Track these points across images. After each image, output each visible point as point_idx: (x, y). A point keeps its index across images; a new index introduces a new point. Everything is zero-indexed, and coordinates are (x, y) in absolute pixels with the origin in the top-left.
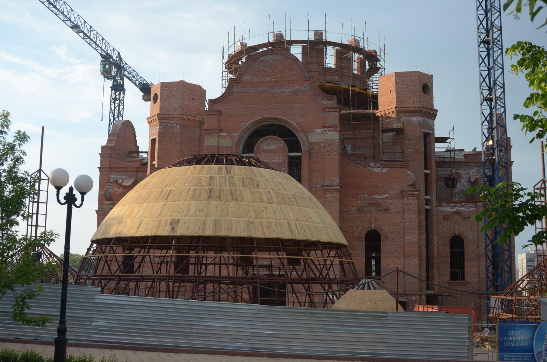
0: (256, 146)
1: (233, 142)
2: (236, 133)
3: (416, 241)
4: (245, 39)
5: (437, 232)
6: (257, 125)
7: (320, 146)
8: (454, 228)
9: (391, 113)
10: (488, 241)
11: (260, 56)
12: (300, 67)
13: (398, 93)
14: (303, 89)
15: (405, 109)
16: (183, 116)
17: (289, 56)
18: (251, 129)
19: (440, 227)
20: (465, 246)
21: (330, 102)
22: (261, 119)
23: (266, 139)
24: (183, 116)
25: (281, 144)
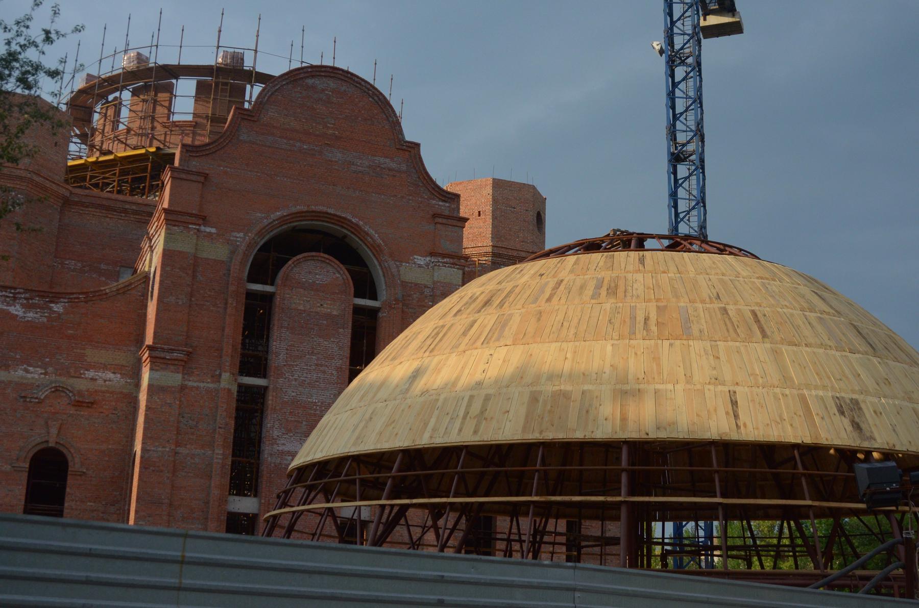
0: (343, 268)
1: (233, 252)
2: (239, 232)
4: (157, 46)
6: (290, 223)
7: (422, 293)
9: (480, 255)
11: (306, 75)
12: (391, 119)
13: (496, 218)
14: (393, 165)
15: (510, 251)
16: (35, 178)
17: (369, 89)
18: (275, 232)
21: (447, 205)
22: (303, 212)
23: (306, 259)
24: (35, 178)
25: (338, 275)
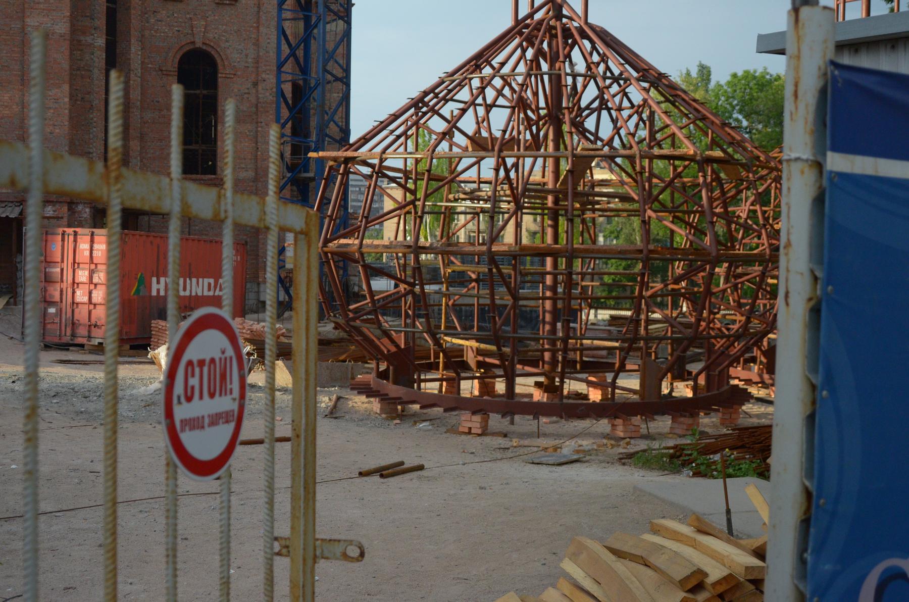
3: (63, 31)
5: (143, 36)
8: (192, 27)
10: (286, 50)
19: (152, 21)
20: (220, 80)
